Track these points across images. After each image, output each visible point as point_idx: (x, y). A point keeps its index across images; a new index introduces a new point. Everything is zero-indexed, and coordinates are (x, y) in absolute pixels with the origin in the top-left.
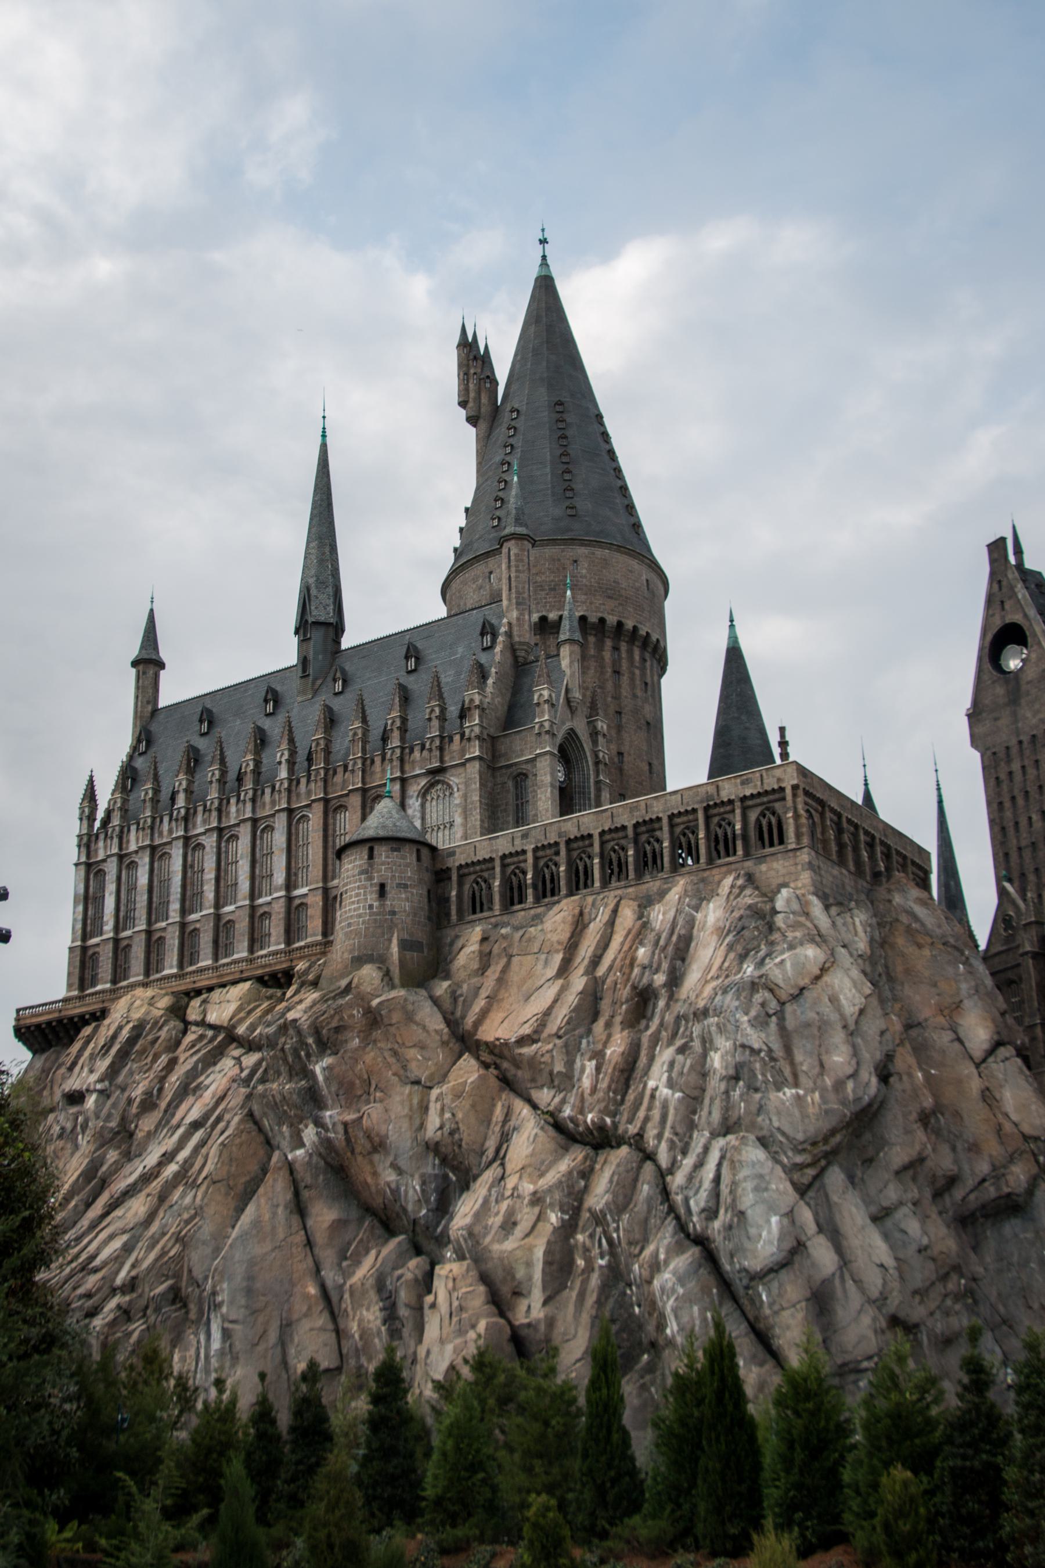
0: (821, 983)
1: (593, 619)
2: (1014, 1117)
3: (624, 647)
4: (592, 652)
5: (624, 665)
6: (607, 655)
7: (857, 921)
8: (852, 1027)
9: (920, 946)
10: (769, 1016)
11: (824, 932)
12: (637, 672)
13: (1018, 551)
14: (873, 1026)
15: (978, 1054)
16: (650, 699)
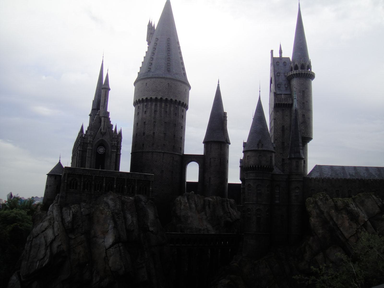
0: (44, 233)
1: (149, 98)
2: (110, 265)
3: (158, 104)
4: (149, 107)
5: (158, 108)
6: (153, 107)
7: (71, 211)
8: (48, 244)
9: (102, 214)
10: (30, 241)
11: (54, 217)
12: (163, 110)
13: (281, 52)
14: (55, 245)
15: (107, 246)
16: (168, 116)
